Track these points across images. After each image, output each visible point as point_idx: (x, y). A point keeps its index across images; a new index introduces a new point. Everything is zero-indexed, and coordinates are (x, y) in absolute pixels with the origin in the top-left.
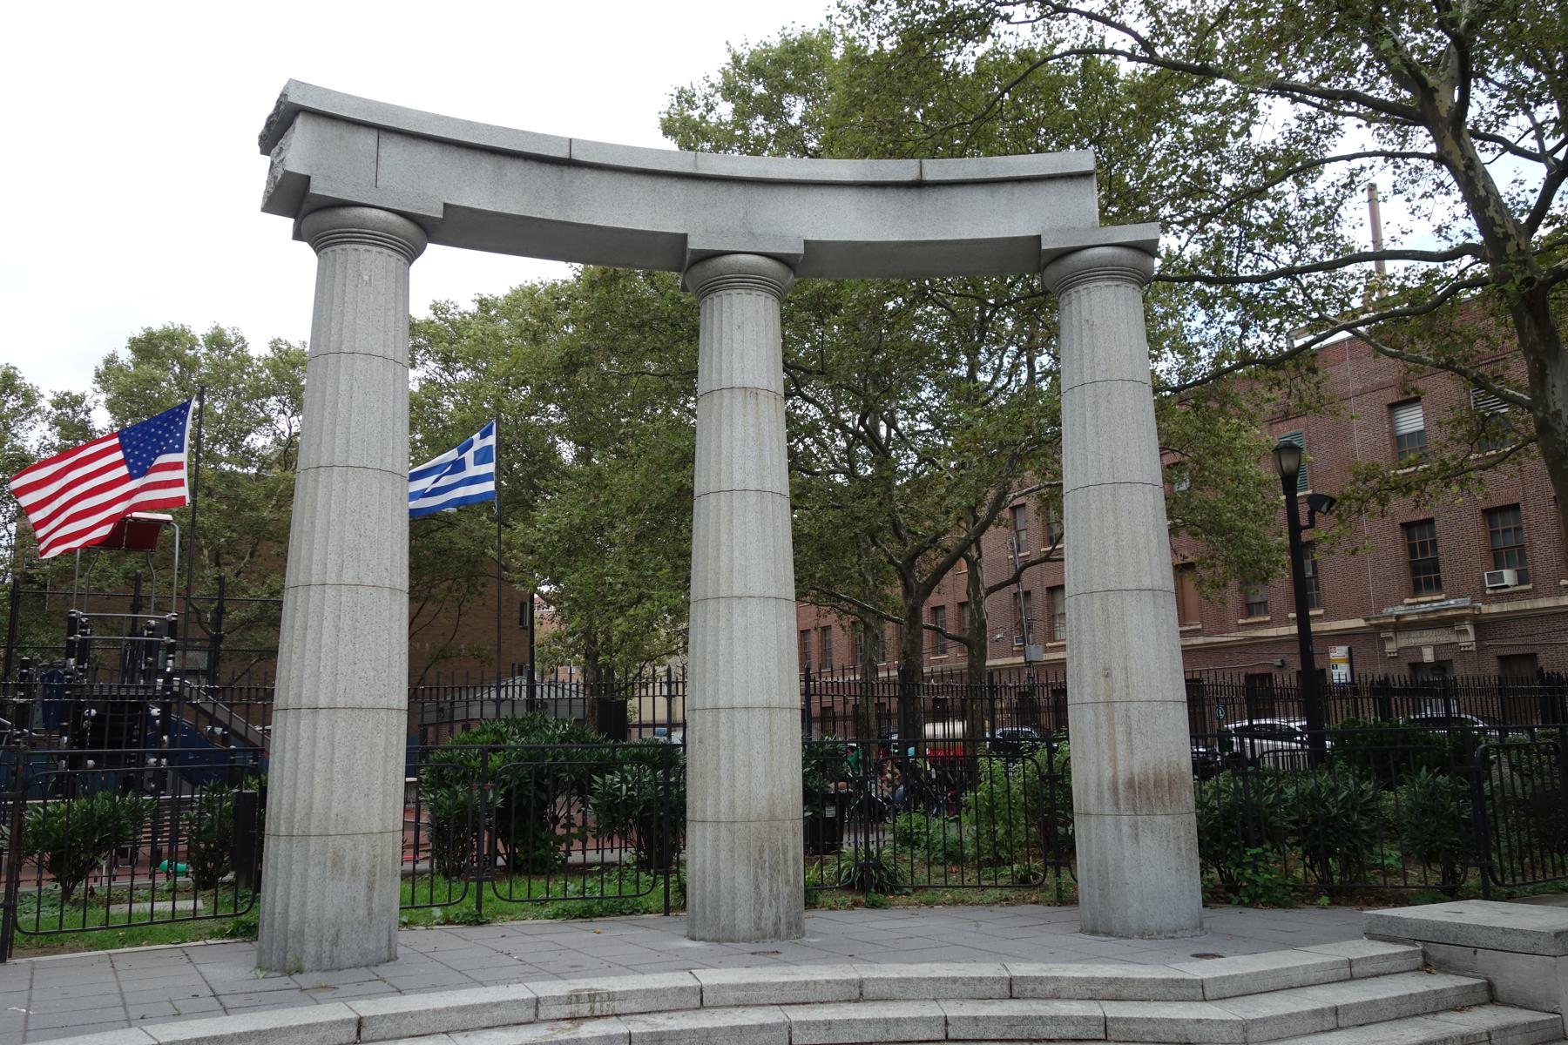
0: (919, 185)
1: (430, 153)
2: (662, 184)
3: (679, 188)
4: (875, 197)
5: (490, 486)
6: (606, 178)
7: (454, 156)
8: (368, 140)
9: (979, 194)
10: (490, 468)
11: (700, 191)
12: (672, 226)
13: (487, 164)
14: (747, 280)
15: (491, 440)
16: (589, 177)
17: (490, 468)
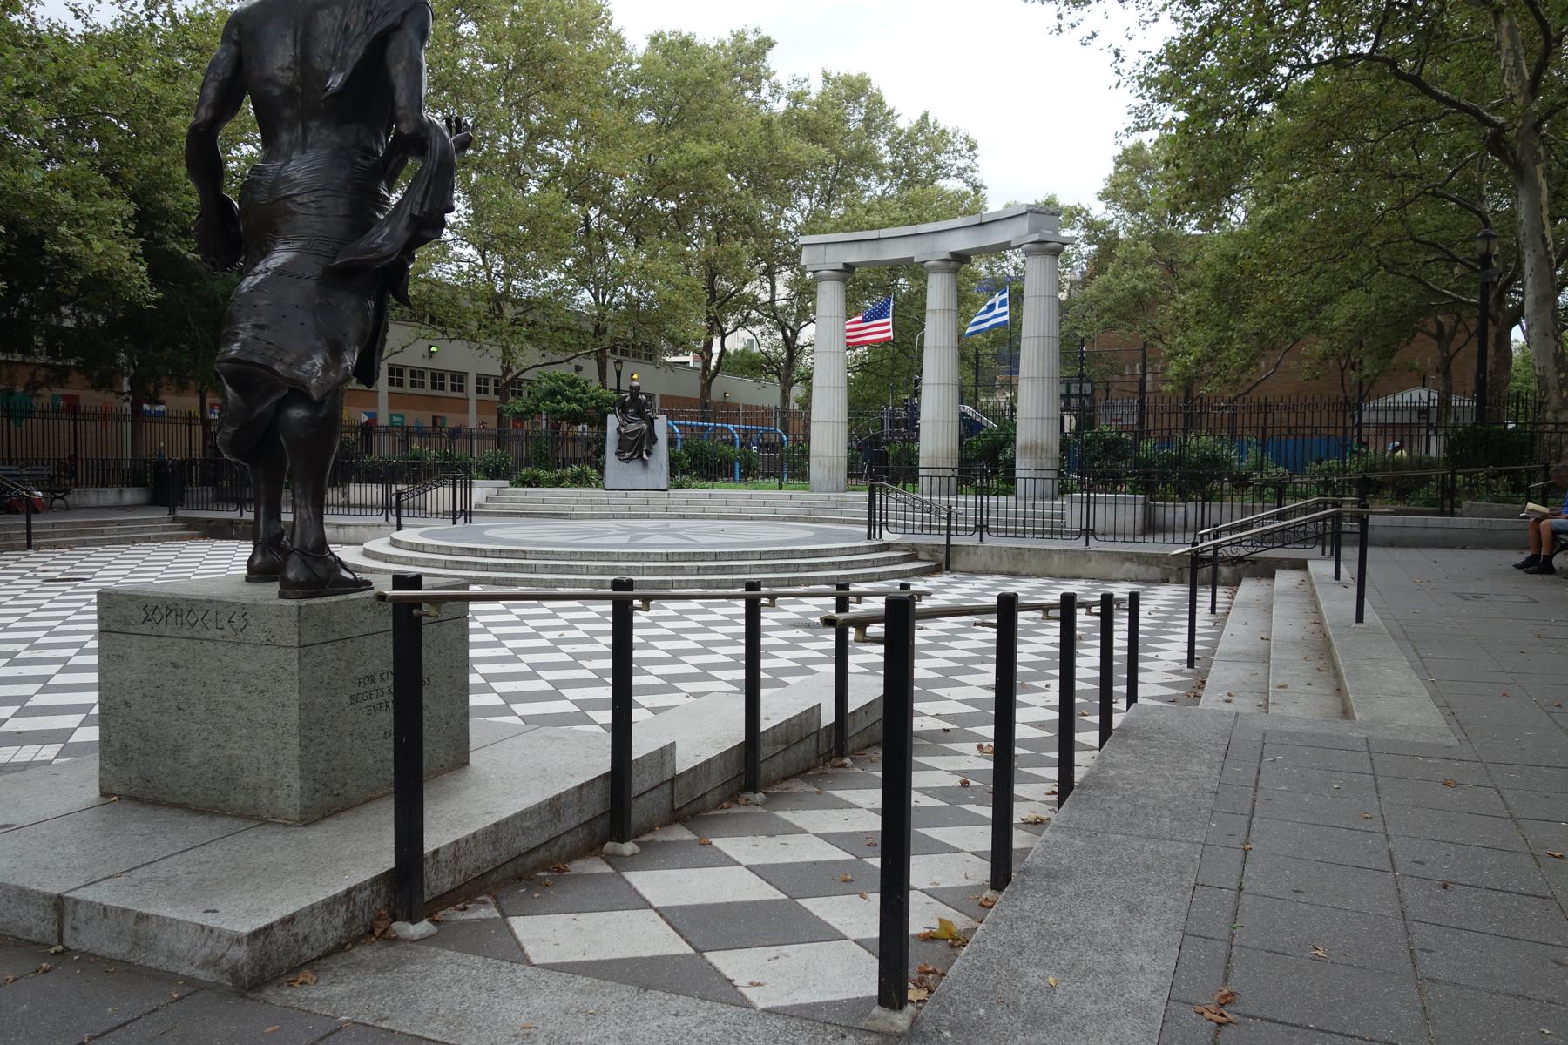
0: (981, 224)
1: (840, 246)
2: (908, 239)
3: (912, 240)
4: (970, 229)
5: (1006, 317)
6: (892, 241)
7: (846, 245)
8: (822, 247)
9: (998, 224)
10: (1006, 309)
11: (919, 238)
12: (910, 255)
13: (856, 245)
14: (934, 269)
15: (1006, 295)
16: (886, 242)
17: (1006, 309)
